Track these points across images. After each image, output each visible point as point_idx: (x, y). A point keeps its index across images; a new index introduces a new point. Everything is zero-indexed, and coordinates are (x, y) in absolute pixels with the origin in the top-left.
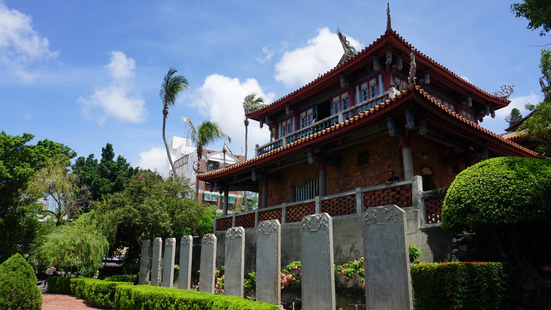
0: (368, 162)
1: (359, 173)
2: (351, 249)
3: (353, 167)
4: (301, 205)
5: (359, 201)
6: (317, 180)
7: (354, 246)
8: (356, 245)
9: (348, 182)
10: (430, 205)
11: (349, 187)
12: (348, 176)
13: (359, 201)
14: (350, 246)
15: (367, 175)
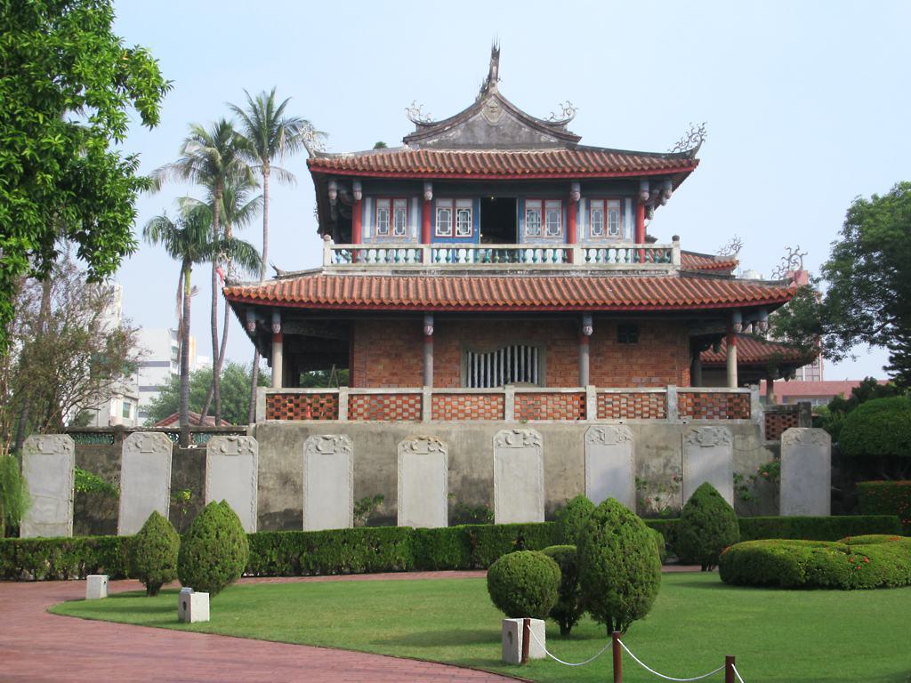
0: (636, 341)
1: (619, 355)
2: (665, 466)
3: (610, 343)
4: (552, 394)
5: (672, 403)
6: (523, 348)
7: (669, 461)
8: (673, 460)
9: (598, 364)
10: (771, 421)
11: (598, 371)
12: (598, 355)
13: (672, 403)
14: (663, 460)
15: (634, 360)
